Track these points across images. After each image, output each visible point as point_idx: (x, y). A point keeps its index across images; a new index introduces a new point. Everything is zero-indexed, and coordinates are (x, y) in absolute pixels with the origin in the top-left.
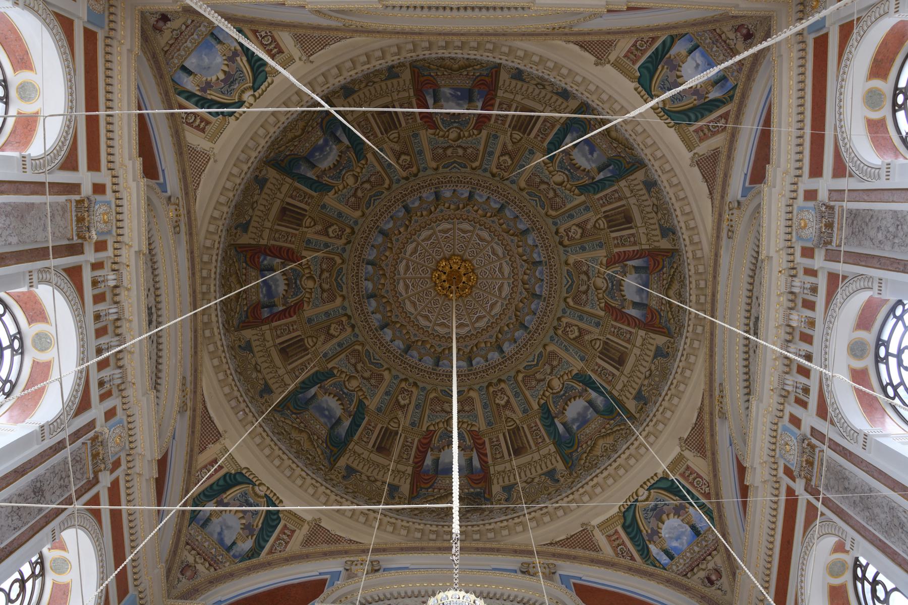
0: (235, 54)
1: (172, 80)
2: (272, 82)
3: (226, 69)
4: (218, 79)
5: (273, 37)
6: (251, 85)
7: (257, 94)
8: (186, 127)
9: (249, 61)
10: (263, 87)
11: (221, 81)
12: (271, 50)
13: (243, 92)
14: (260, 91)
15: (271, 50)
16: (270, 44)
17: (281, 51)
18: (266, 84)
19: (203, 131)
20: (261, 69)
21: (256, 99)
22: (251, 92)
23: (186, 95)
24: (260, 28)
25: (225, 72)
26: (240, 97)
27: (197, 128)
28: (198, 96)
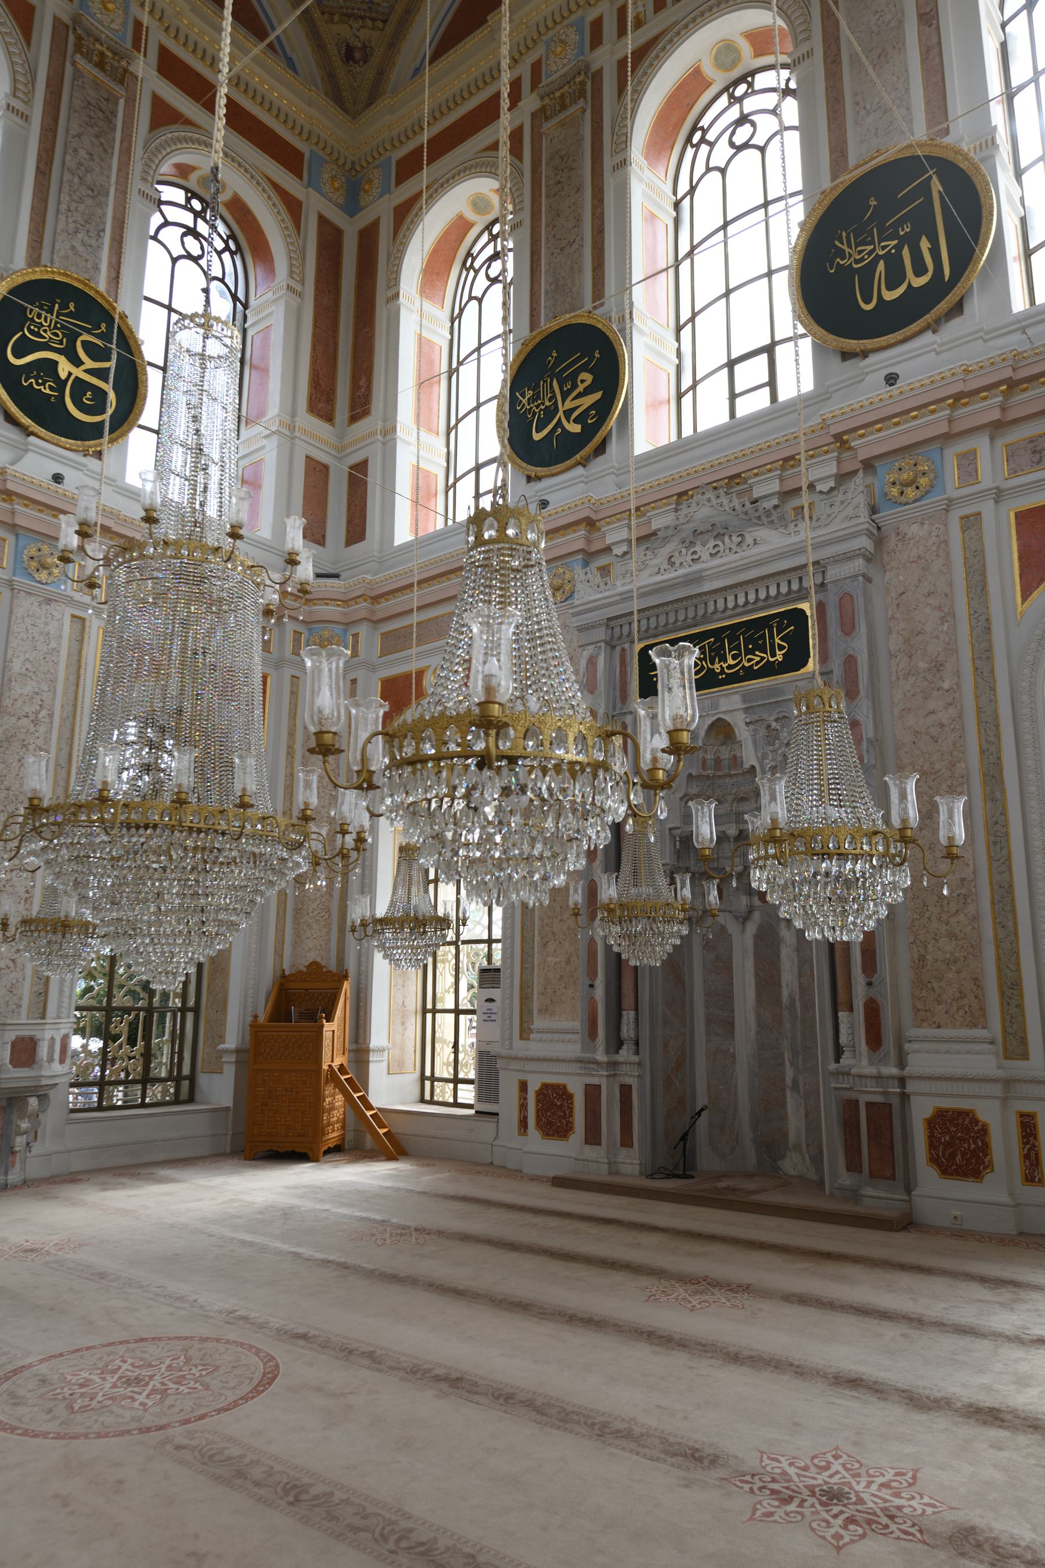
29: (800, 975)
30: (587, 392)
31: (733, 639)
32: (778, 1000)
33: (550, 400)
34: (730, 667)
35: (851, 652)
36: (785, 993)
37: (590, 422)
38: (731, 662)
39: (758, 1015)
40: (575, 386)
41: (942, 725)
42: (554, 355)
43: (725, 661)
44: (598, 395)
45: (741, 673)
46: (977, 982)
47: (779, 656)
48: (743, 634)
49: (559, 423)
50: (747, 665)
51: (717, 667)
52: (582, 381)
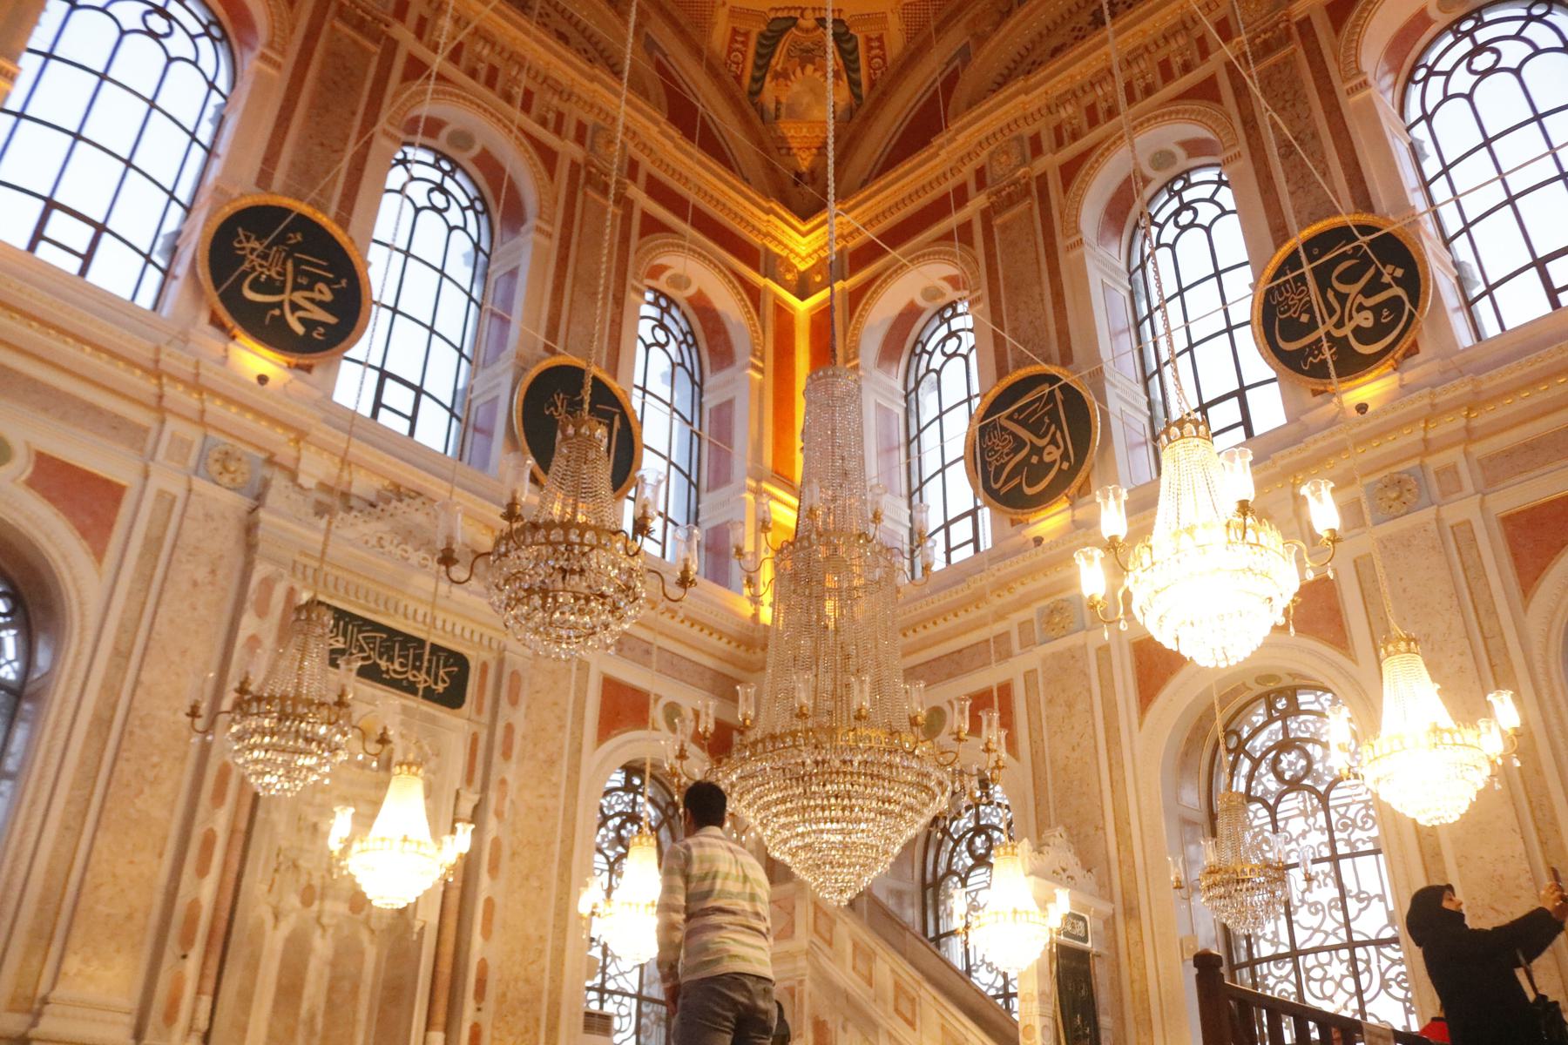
0: (777, 76)
1: (851, 117)
2: (772, 9)
3: (798, 71)
4: (815, 70)
5: (729, 53)
6: (793, 29)
7: (797, 14)
8: (889, 60)
9: (772, 55)
10: (785, 14)
11: (813, 63)
12: (742, 43)
13: (807, 31)
14: (792, 14)
15: (742, 43)
16: (738, 50)
17: (735, 31)
18: (780, 14)
19: (880, 39)
20: (769, 34)
21: (803, 10)
22: (801, 22)
23: (856, 90)
24: (730, 80)
25: (803, 69)
26: (815, 29)
27: (881, 47)
28: (849, 77)
29: (332, 989)
30: (321, 305)
31: (403, 647)
32: (297, 1015)
33: (279, 274)
34: (395, 671)
35: (511, 720)
36: (305, 1006)
37: (315, 335)
38: (397, 667)
39: (270, 1026)
40: (310, 288)
41: (546, 810)
42: (299, 237)
43: (393, 663)
44: (331, 320)
45: (405, 683)
46: (538, 1020)
47: (440, 687)
48: (415, 648)
49: (280, 305)
50: (411, 678)
51: (383, 664)
52: (321, 292)
